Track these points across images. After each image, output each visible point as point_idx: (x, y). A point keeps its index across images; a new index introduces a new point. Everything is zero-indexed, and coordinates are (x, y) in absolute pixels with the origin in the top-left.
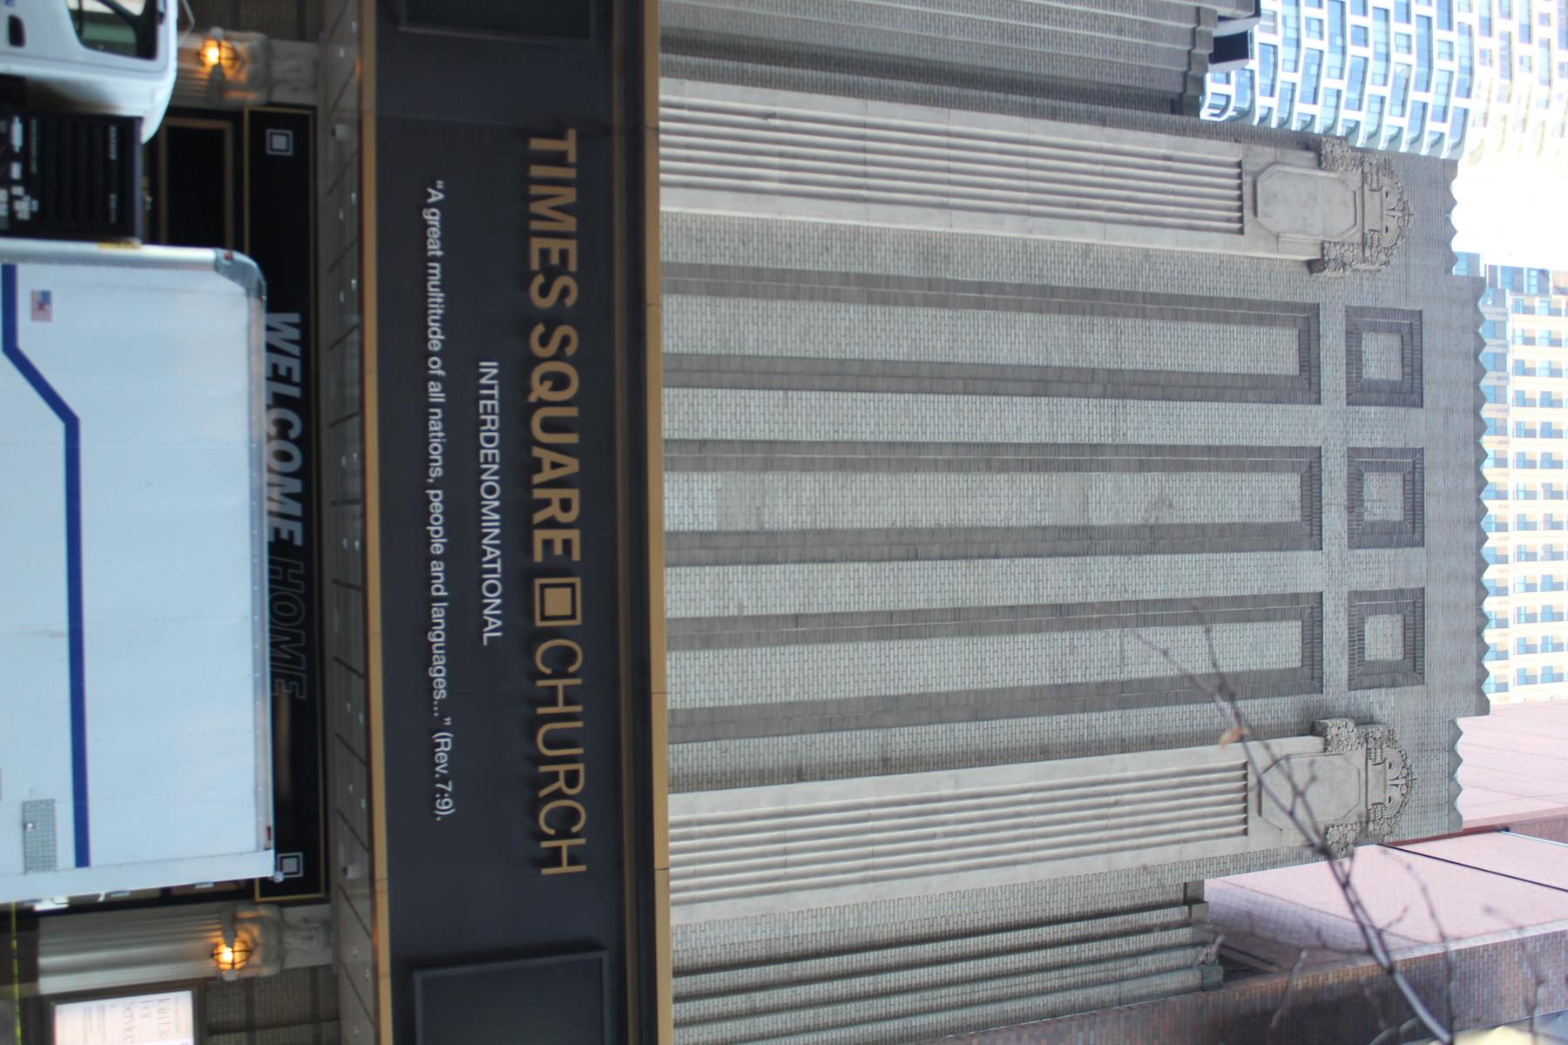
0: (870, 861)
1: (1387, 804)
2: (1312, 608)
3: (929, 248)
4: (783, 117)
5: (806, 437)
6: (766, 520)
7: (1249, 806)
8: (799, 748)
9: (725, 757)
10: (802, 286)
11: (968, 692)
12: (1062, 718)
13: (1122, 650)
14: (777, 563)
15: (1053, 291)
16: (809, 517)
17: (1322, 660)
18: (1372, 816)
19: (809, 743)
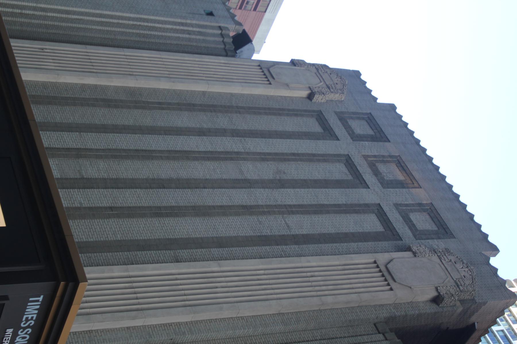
0: (185, 297)
1: (464, 279)
2: (377, 209)
3: (131, 91)
4: (49, 49)
5: (93, 147)
6: (84, 174)
7: (387, 278)
8: (130, 257)
9: (90, 260)
10: (77, 102)
11: (212, 237)
12: (268, 248)
13: (286, 223)
14: (94, 188)
15: (194, 105)
16: (105, 174)
17: (394, 228)
18: (459, 283)
19: (134, 255)
